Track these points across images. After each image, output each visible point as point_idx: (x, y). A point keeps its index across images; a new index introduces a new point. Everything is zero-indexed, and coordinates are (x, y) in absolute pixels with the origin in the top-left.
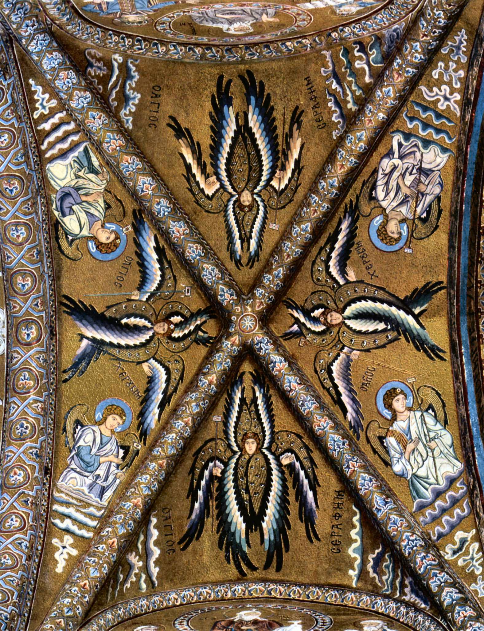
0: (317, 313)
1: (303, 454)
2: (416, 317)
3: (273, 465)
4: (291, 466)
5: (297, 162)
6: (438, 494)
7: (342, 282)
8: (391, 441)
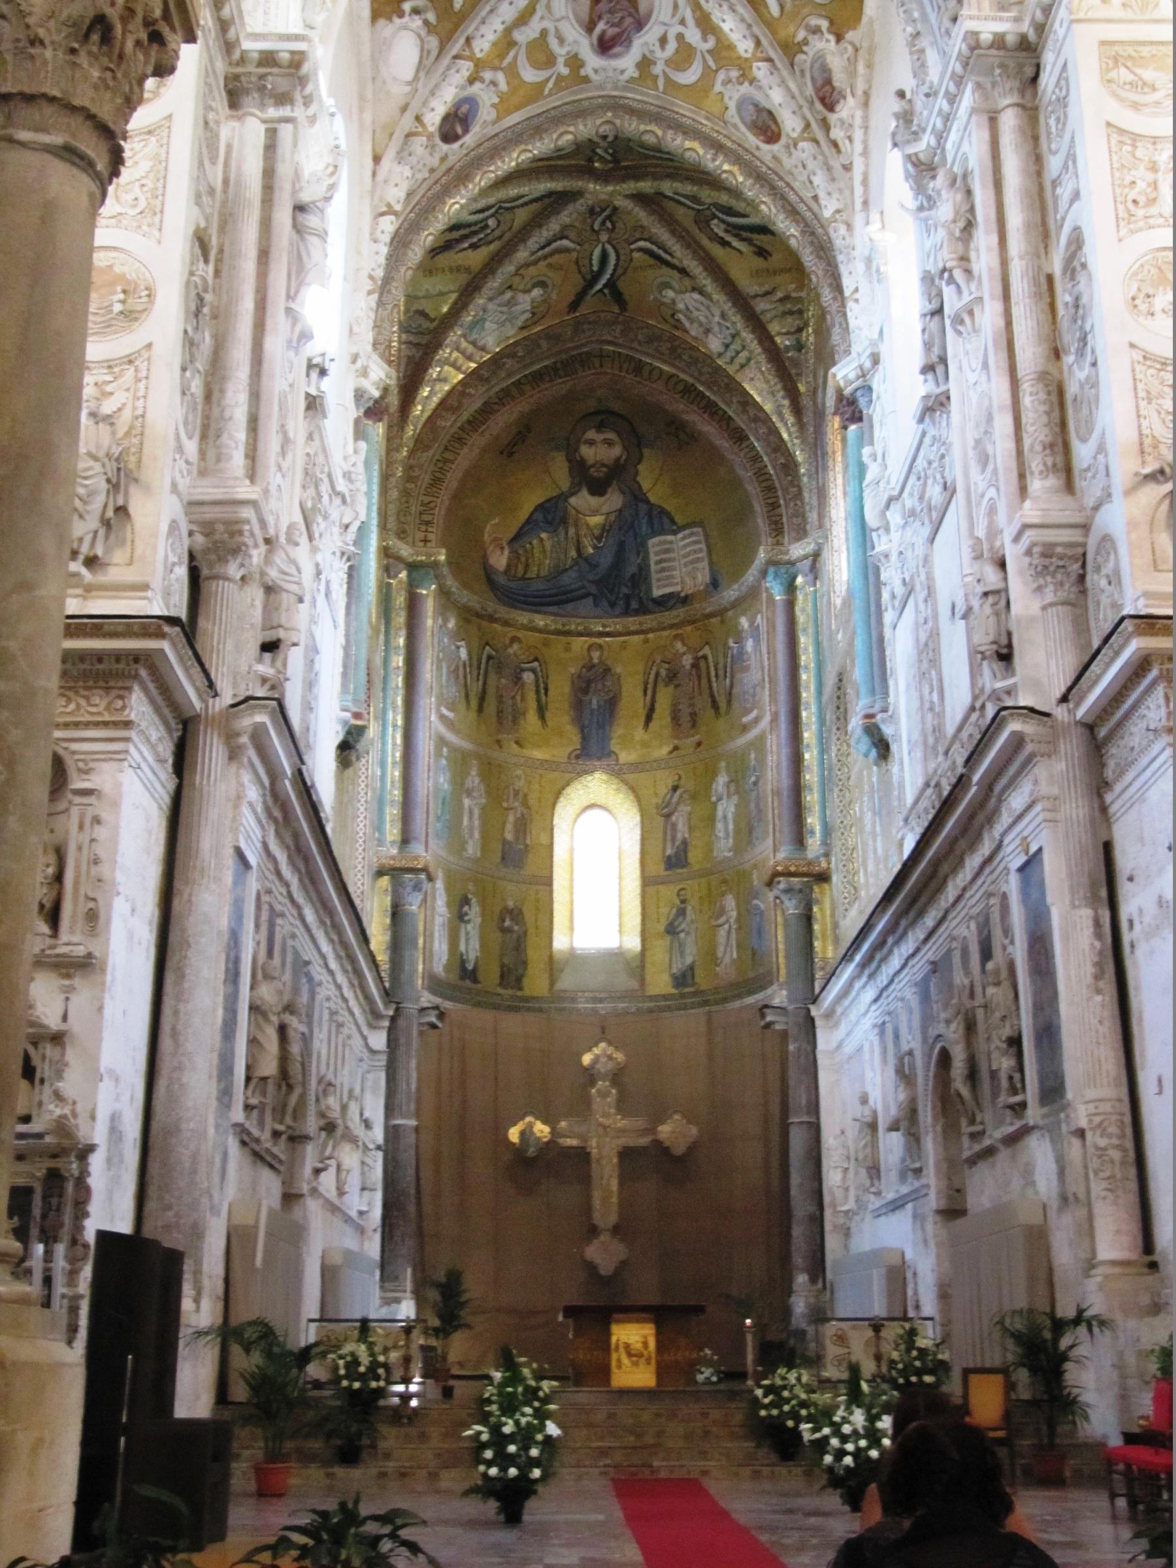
0: (609, 224)
1: (497, 233)
2: (601, 290)
3: (487, 213)
4: (487, 226)
6: (474, 343)
8: (508, 295)
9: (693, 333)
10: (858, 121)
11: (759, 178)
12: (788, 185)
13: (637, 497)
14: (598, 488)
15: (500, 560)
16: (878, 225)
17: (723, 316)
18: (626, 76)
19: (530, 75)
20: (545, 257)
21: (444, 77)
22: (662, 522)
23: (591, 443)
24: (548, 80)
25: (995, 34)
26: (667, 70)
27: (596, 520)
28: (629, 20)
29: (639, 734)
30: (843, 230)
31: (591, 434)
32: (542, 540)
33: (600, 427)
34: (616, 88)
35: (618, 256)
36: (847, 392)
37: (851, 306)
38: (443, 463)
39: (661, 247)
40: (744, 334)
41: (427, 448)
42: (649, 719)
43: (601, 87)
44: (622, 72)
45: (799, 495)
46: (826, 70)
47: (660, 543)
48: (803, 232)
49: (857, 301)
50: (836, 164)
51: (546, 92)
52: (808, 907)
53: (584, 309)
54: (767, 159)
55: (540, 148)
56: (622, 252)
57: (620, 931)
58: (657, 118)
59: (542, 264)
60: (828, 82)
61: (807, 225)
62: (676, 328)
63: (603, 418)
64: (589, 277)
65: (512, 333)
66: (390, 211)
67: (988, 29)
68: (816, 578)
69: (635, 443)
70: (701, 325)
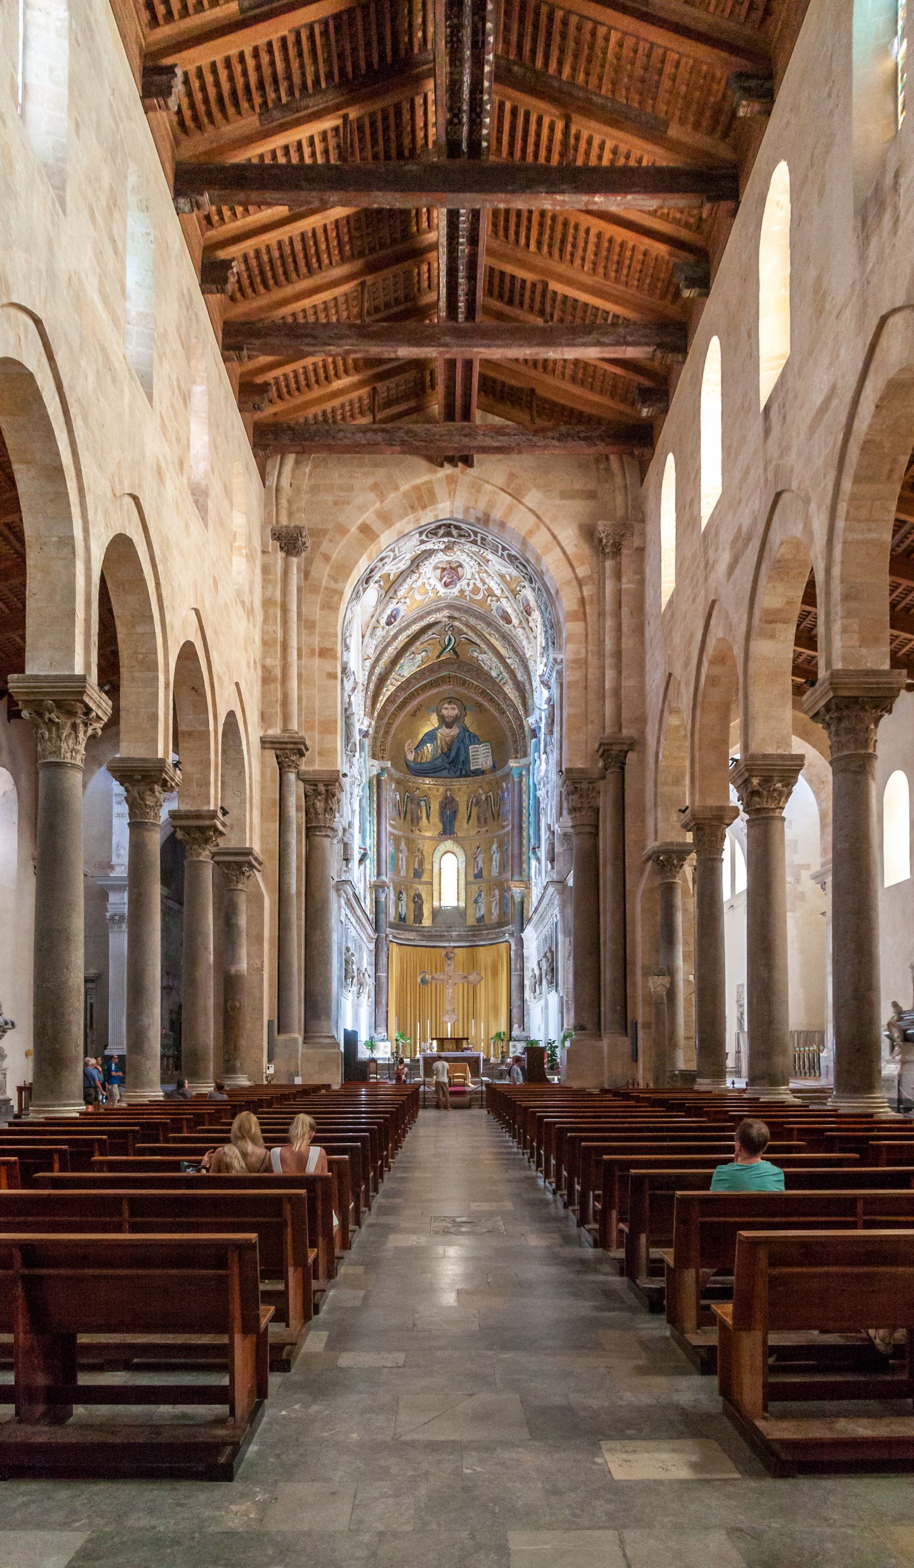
13: (465, 729)
15: (411, 757)
19: (418, 597)
21: (387, 605)
22: (475, 739)
29: (465, 826)
31: (446, 706)
33: (450, 703)
38: (389, 725)
42: (469, 819)
46: (527, 600)
50: (531, 637)
53: (442, 658)
63: (450, 700)
65: (414, 669)
66: (369, 658)
69: (463, 708)
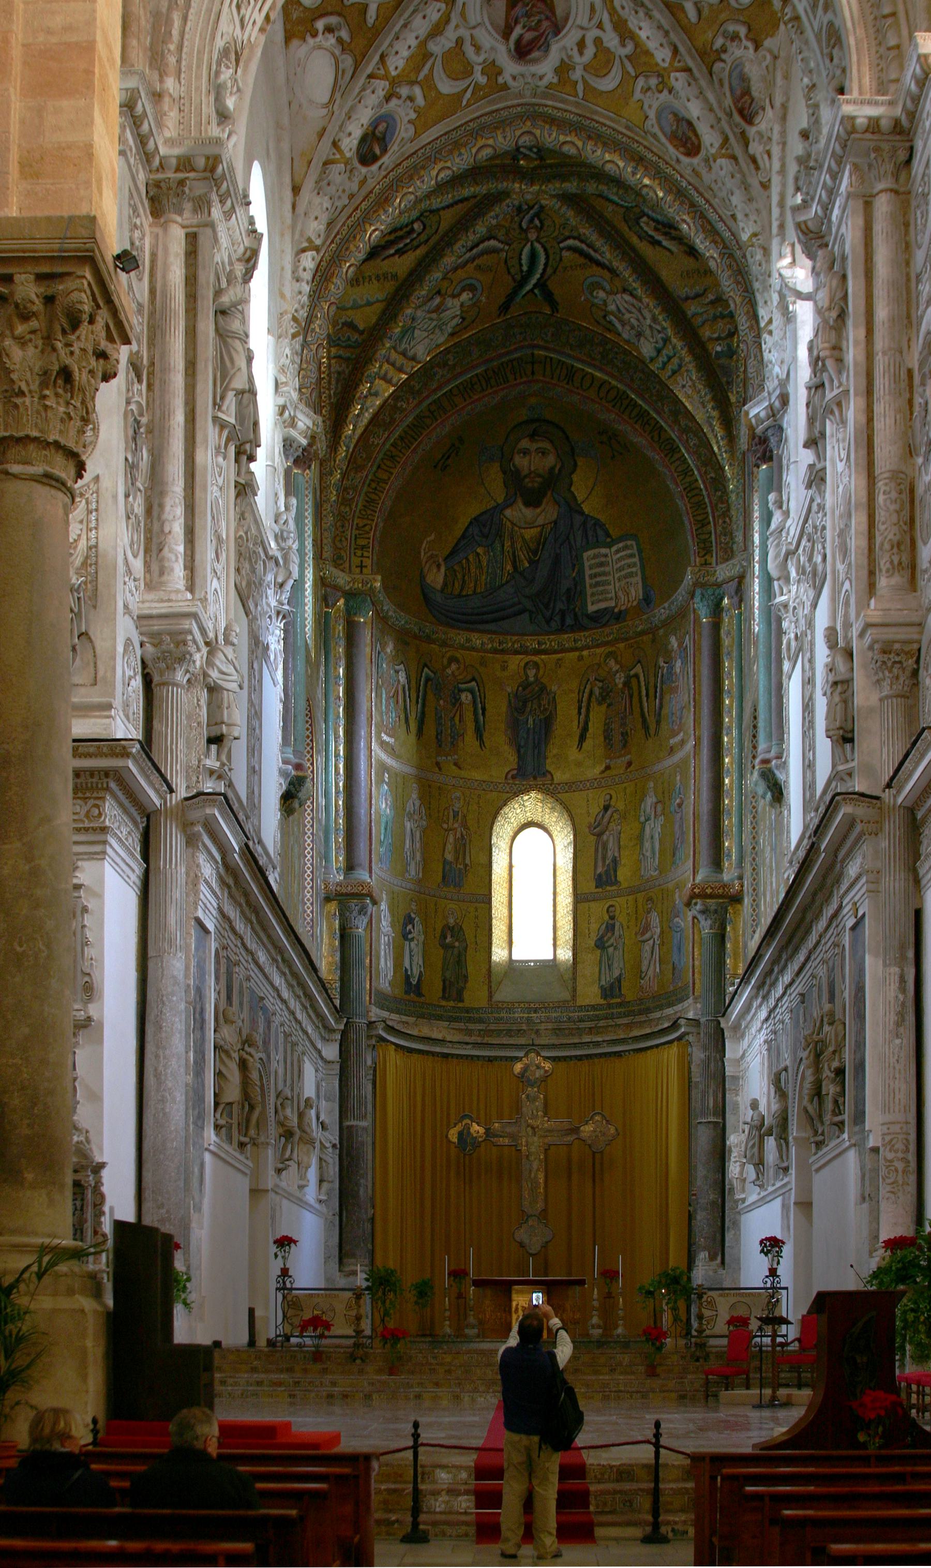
5: (659, 243)
7: (562, 245)
9: (625, 336)
10: (776, 136)
11: (680, 194)
12: (707, 201)
13: (572, 508)
14: (533, 500)
16: (788, 260)
17: (654, 319)
18: (545, 82)
19: (446, 87)
20: (473, 259)
23: (525, 452)
24: (466, 90)
25: (870, 118)
26: (587, 76)
27: (529, 534)
28: (545, 24)
30: (759, 257)
31: (525, 443)
32: (478, 554)
33: (533, 436)
34: (535, 95)
35: (547, 258)
36: (759, 430)
37: (765, 336)
39: (590, 246)
40: (674, 340)
41: (359, 469)
43: (520, 95)
44: (541, 78)
45: (726, 513)
47: (595, 557)
48: (722, 255)
49: (770, 333)
51: (464, 103)
52: (723, 928)
54: (687, 172)
55: (460, 162)
56: (551, 252)
57: (555, 945)
58: (576, 128)
59: (470, 267)
60: (747, 92)
61: (725, 247)
62: (610, 331)
64: (518, 277)
67: (864, 113)
68: (741, 601)
70: (633, 328)
